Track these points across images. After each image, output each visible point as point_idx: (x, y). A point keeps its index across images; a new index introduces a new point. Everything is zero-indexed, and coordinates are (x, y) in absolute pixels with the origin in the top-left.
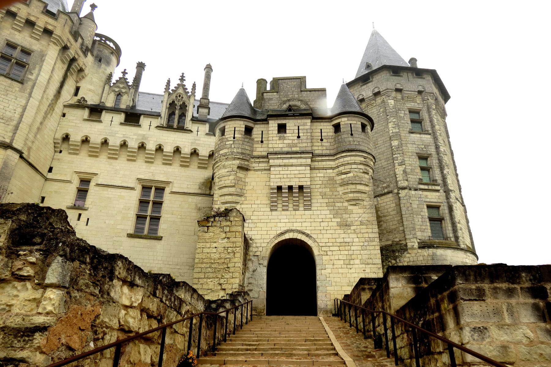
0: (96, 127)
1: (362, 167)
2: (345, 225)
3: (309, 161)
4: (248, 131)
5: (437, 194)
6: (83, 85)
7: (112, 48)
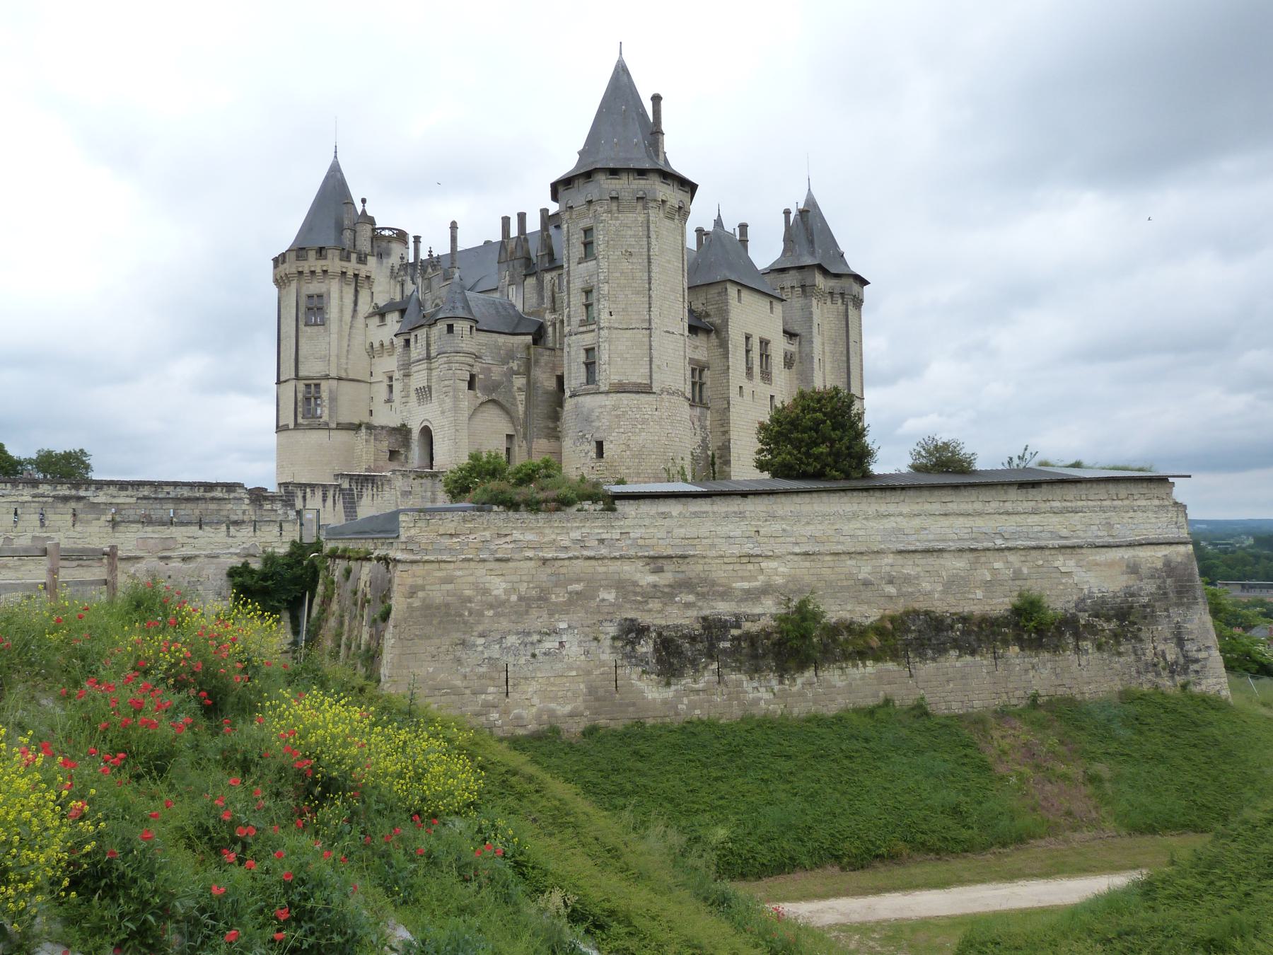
0: (386, 329)
1: (446, 366)
2: (443, 412)
3: (425, 366)
4: (407, 342)
5: (593, 334)
6: (376, 289)
7: (390, 236)
